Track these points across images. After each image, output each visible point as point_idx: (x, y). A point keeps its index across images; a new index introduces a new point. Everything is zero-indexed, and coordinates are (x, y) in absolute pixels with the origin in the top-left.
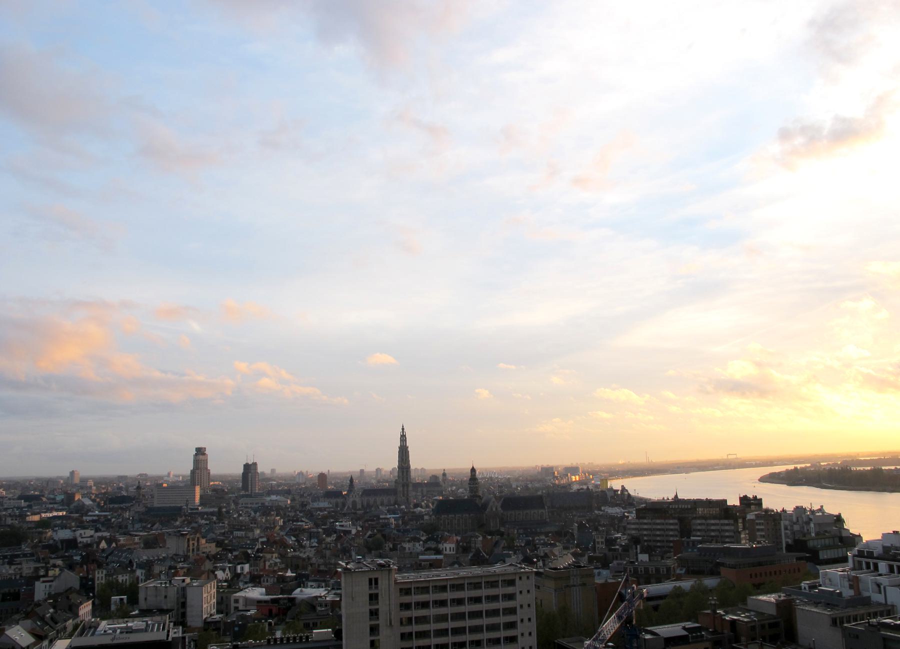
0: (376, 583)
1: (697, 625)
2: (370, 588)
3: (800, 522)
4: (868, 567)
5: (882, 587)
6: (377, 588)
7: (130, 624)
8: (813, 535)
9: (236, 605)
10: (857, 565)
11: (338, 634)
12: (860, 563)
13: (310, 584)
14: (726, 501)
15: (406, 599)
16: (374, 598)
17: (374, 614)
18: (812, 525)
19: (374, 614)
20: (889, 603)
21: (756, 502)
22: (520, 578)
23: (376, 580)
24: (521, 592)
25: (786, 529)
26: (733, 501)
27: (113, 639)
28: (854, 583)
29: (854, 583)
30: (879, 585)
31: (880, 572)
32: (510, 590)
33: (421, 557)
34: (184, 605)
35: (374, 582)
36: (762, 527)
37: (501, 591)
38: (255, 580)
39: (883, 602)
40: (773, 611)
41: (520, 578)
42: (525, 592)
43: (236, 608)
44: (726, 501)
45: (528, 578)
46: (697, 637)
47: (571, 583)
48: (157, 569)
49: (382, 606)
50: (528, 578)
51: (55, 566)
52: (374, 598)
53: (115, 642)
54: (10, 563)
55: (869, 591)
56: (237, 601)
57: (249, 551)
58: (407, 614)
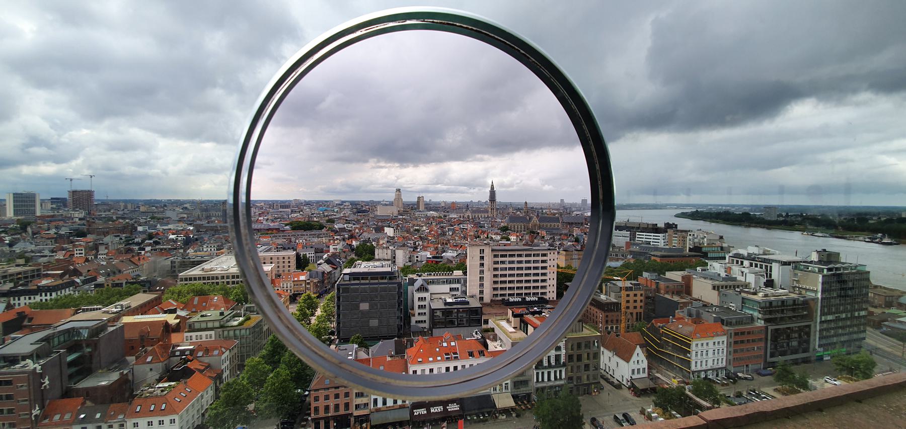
0: (483, 252)
1: (637, 283)
2: (480, 254)
3: (699, 238)
4: (737, 262)
5: (744, 273)
6: (483, 254)
7: (375, 264)
8: (705, 245)
9: (417, 259)
10: (730, 262)
11: (465, 273)
12: (733, 260)
13: (449, 251)
14: (657, 224)
15: (496, 259)
16: (482, 258)
17: (482, 265)
18: (705, 240)
19: (482, 265)
20: (747, 281)
21: (674, 226)
22: (550, 253)
23: (483, 250)
24: (550, 260)
25: (690, 240)
26: (661, 225)
27: (369, 270)
28: (728, 270)
29: (728, 270)
30: (742, 272)
31: (744, 266)
32: (544, 258)
33: (500, 242)
34: (394, 258)
35: (482, 251)
36: (674, 238)
37: (540, 258)
38: (425, 248)
39: (744, 280)
40: (680, 280)
41: (550, 253)
42: (552, 260)
43: (417, 260)
44: (657, 224)
45: (554, 253)
46: (637, 288)
47: (573, 257)
48: (381, 242)
49: (486, 262)
50: (554, 253)
51: (337, 239)
52: (482, 258)
53: (370, 271)
54: (318, 237)
55: (736, 274)
56: (417, 257)
57: (422, 236)
58: (496, 266)
